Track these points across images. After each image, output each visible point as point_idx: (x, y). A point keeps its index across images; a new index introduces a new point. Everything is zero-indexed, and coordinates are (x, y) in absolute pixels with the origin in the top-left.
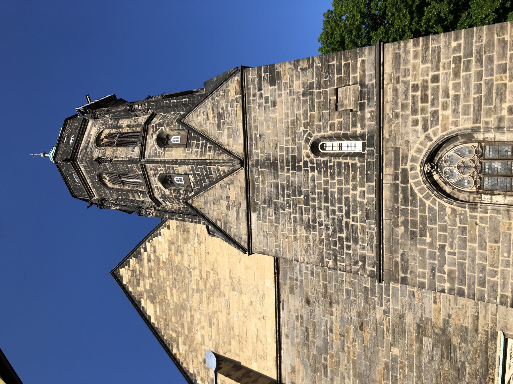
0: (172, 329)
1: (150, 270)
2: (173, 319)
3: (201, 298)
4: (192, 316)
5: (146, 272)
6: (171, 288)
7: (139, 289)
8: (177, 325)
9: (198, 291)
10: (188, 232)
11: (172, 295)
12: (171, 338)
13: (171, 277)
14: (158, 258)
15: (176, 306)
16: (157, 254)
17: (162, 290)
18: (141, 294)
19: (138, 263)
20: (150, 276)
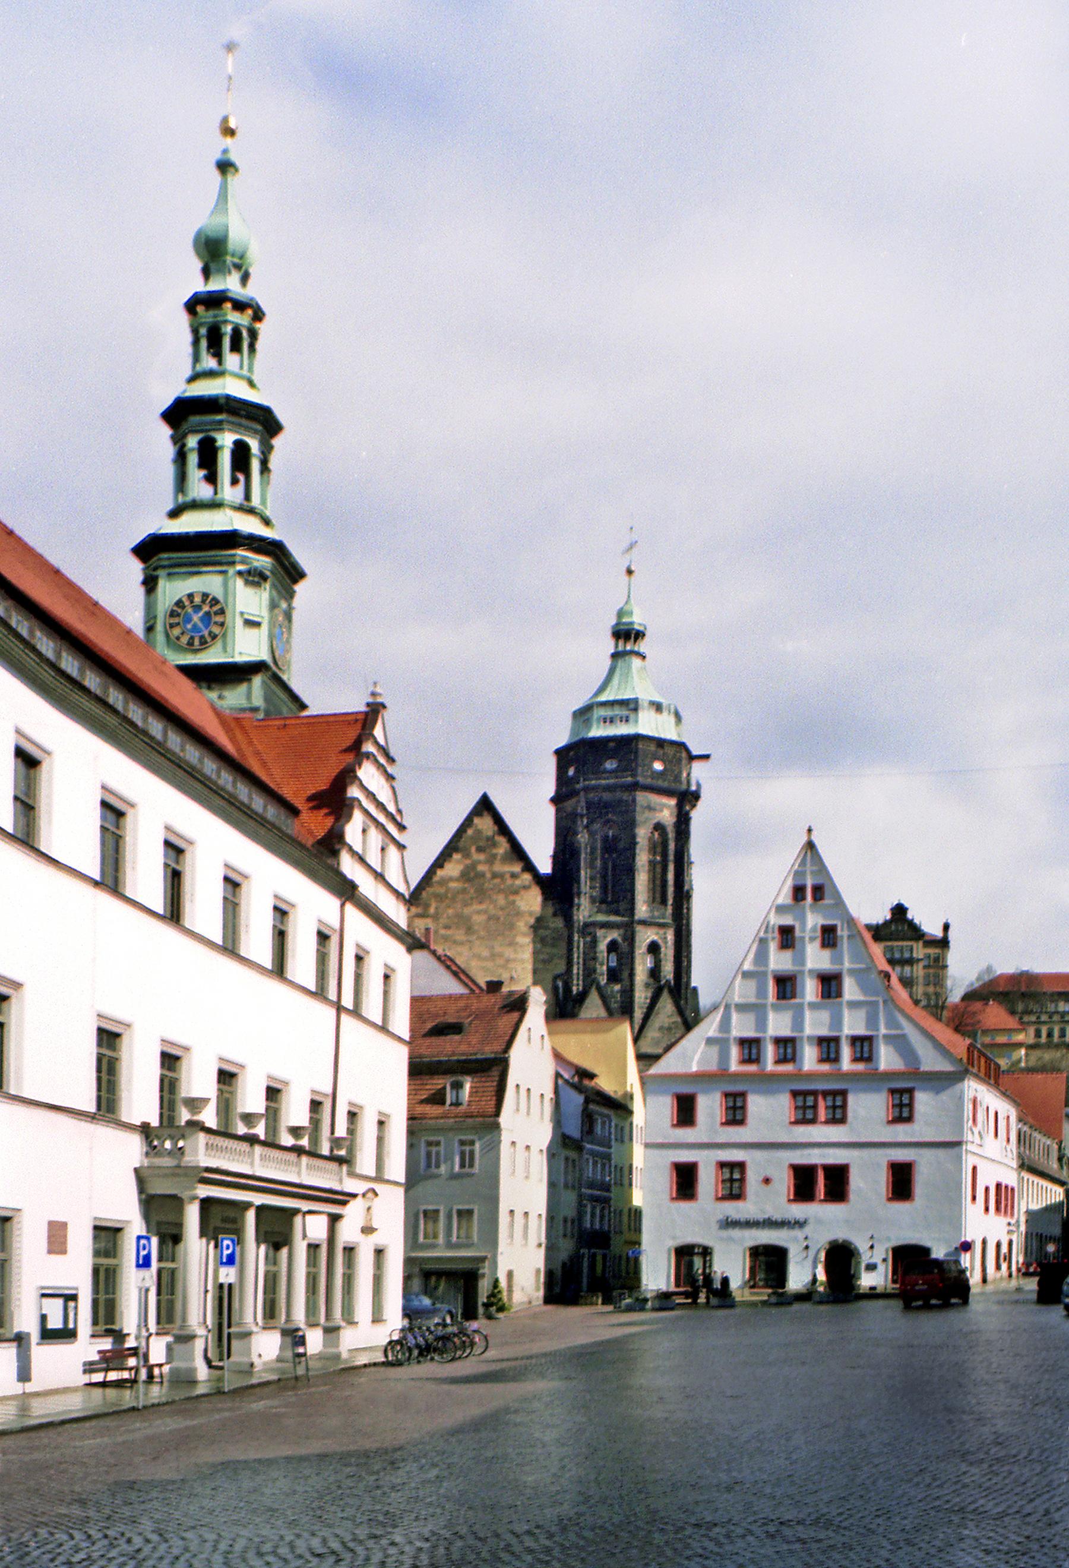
0: (436, 908)
1: (501, 876)
2: (450, 911)
3: (485, 959)
4: (462, 944)
5: (498, 867)
6: (485, 912)
7: (473, 849)
8: (445, 915)
9: (493, 956)
10: (553, 946)
11: (478, 912)
12: (427, 906)
13: (501, 913)
14: (516, 893)
15: (468, 919)
16: (522, 893)
17: (482, 894)
18: (467, 855)
19: (506, 853)
20: (495, 876)
